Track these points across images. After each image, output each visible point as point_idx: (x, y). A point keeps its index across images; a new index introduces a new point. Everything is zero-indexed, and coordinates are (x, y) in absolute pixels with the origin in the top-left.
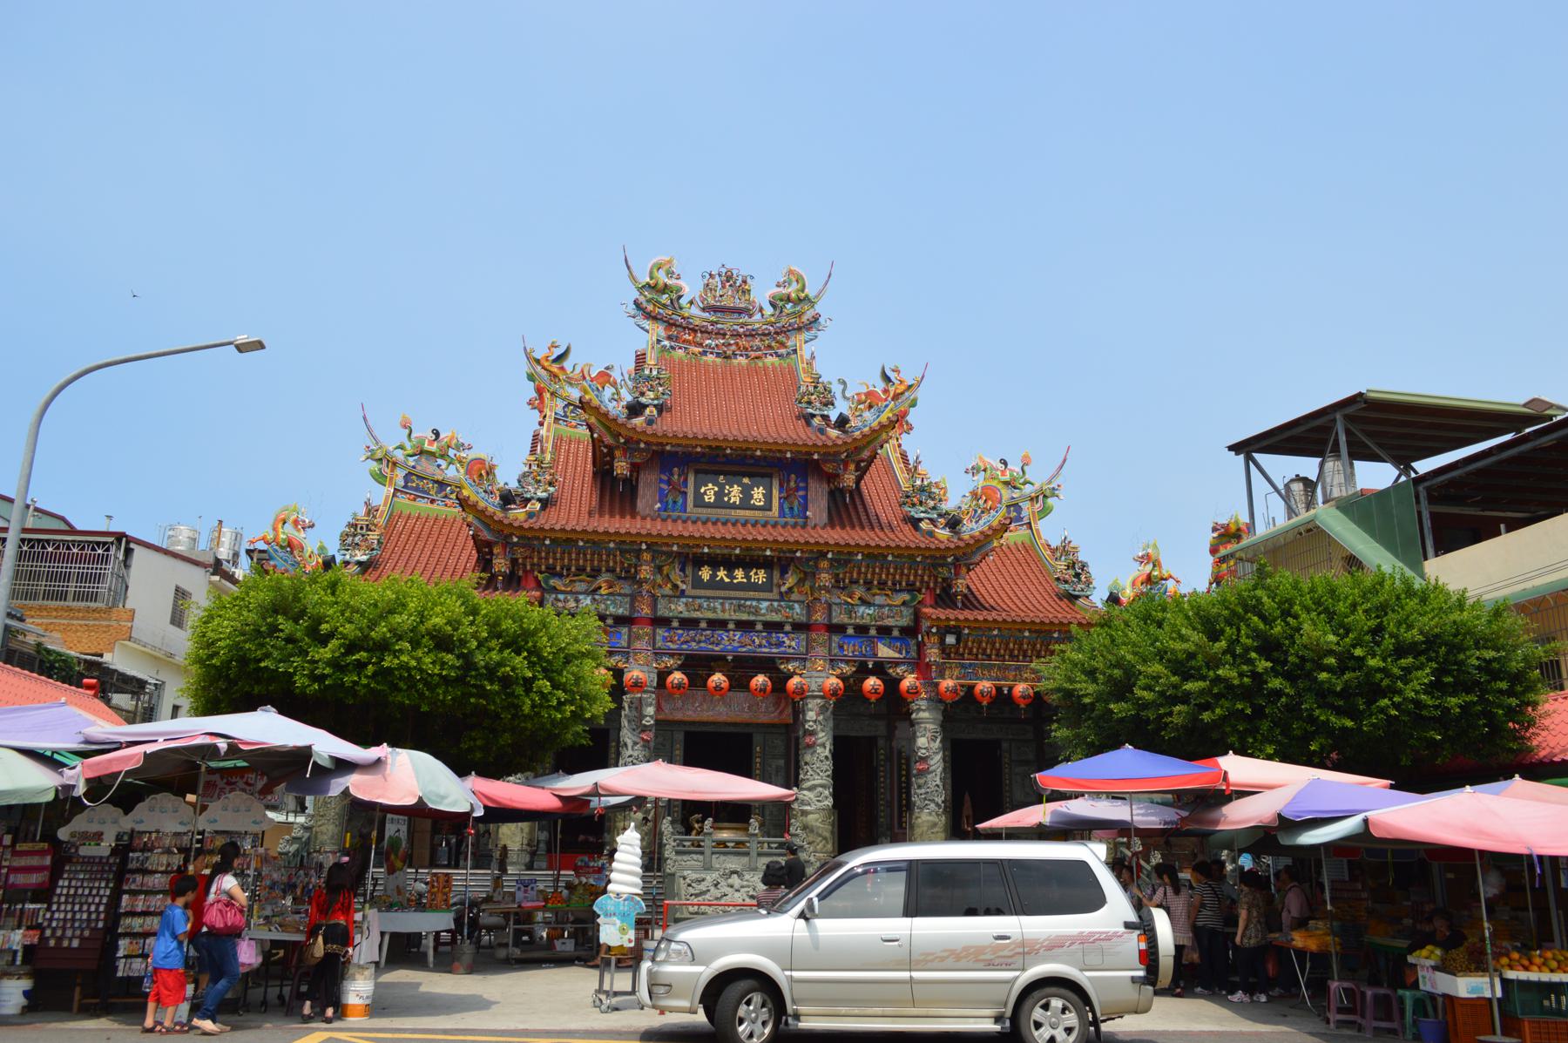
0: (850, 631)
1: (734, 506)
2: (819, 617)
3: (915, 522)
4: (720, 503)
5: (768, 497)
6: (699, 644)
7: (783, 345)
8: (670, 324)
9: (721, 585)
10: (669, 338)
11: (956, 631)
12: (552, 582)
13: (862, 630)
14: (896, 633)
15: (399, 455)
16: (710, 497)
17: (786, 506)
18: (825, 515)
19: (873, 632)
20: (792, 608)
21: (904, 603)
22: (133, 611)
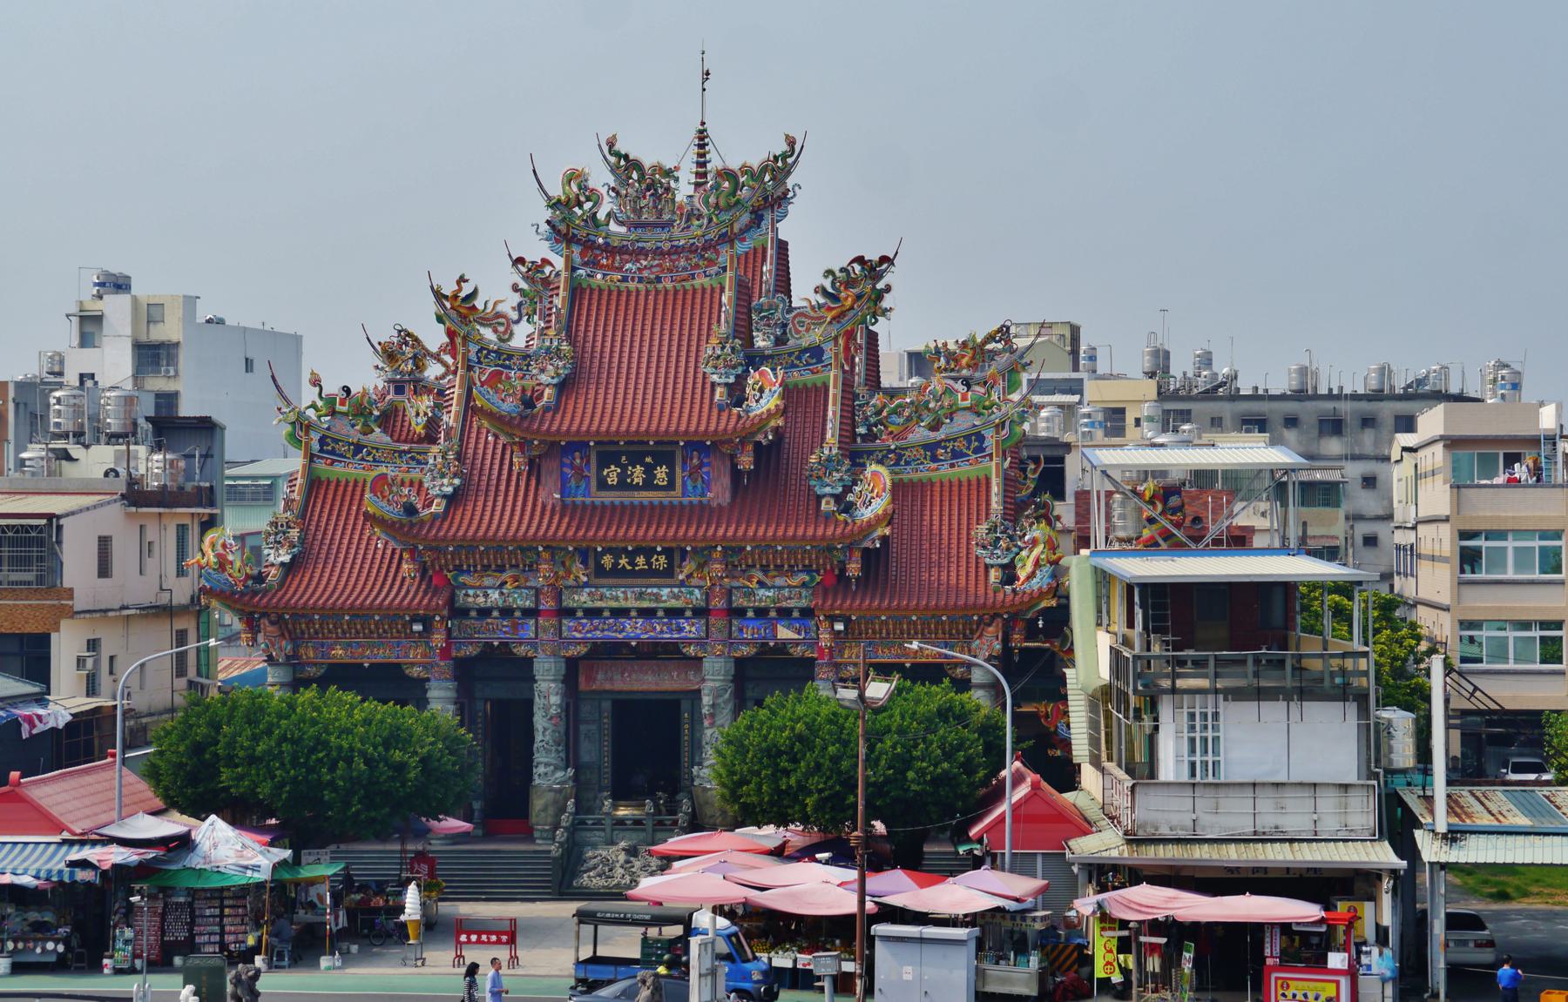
0: (750, 614)
1: (637, 488)
2: (718, 603)
3: (819, 498)
4: (624, 485)
5: (671, 476)
6: (603, 632)
7: (711, 262)
8: (588, 245)
9: (623, 573)
10: (585, 264)
11: (847, 621)
12: (461, 579)
13: (761, 613)
14: (796, 614)
15: (311, 413)
16: (613, 479)
17: (689, 483)
18: (728, 495)
19: (773, 614)
20: (691, 593)
21: (804, 585)
22: (71, 590)
